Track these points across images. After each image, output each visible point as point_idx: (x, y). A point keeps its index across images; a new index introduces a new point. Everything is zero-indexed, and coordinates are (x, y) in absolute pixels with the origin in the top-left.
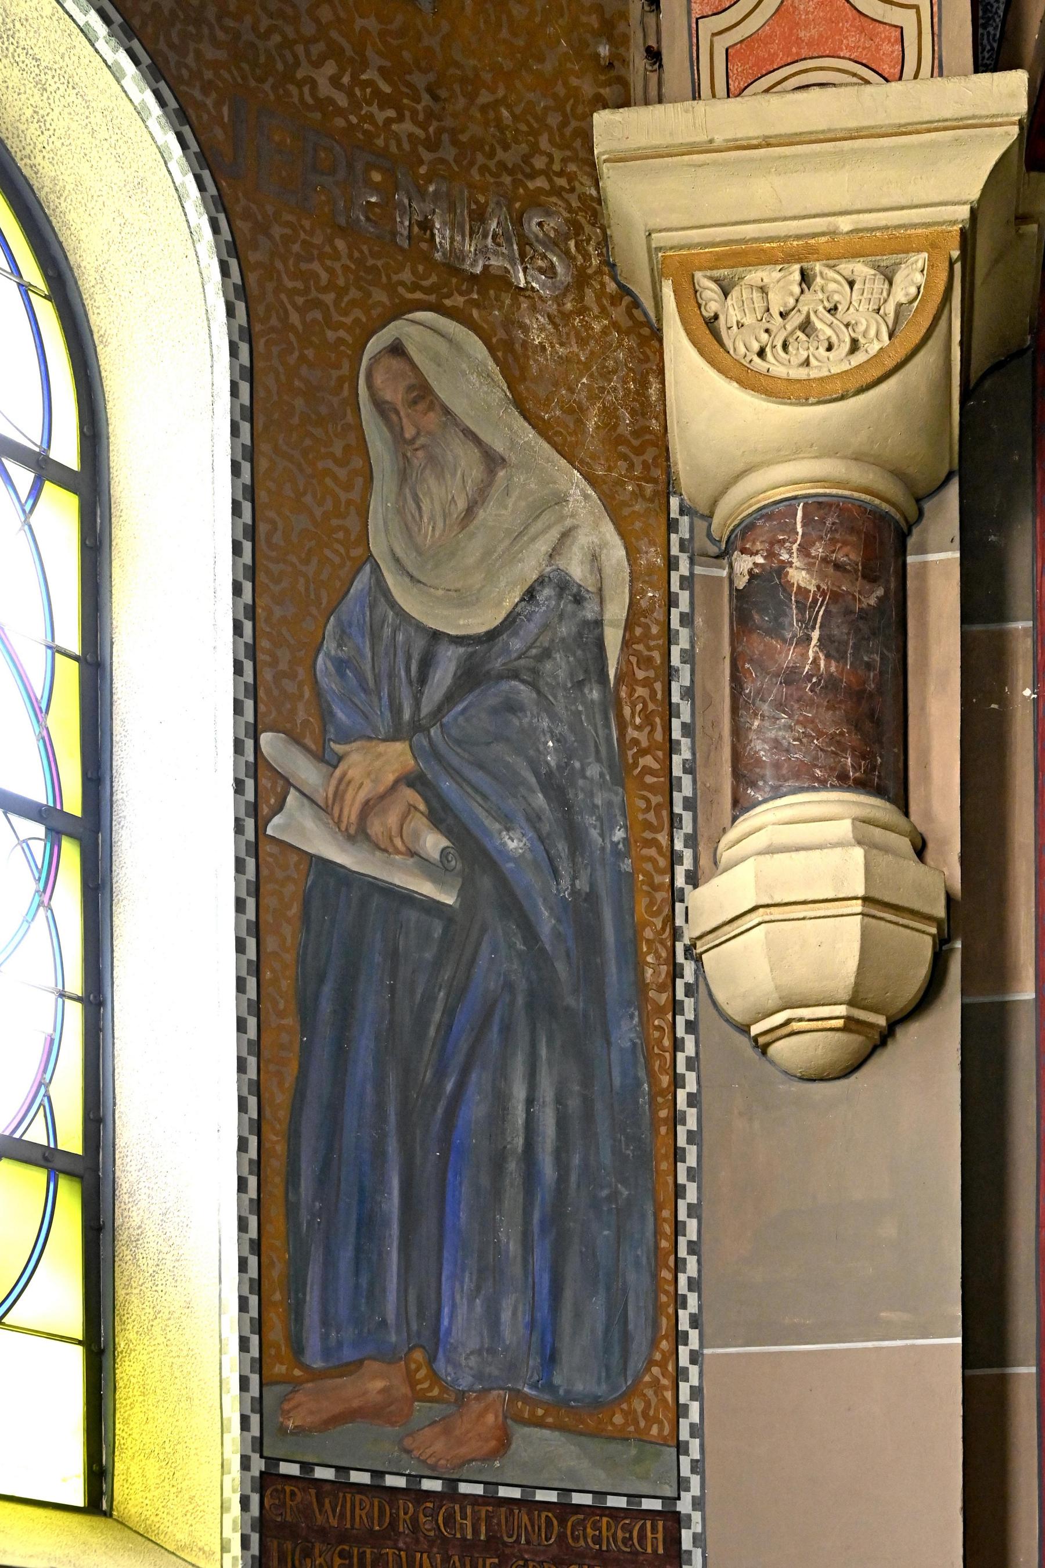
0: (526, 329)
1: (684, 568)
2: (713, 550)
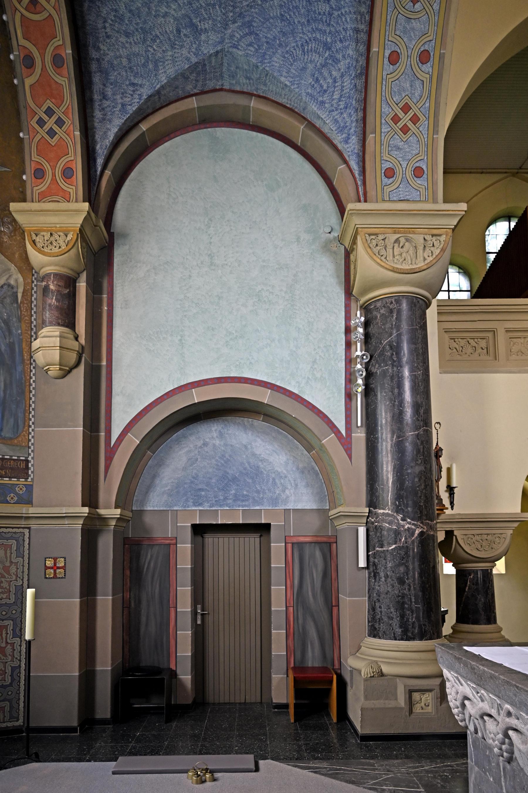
0: (3, 238)
1: (35, 283)
2: (41, 280)
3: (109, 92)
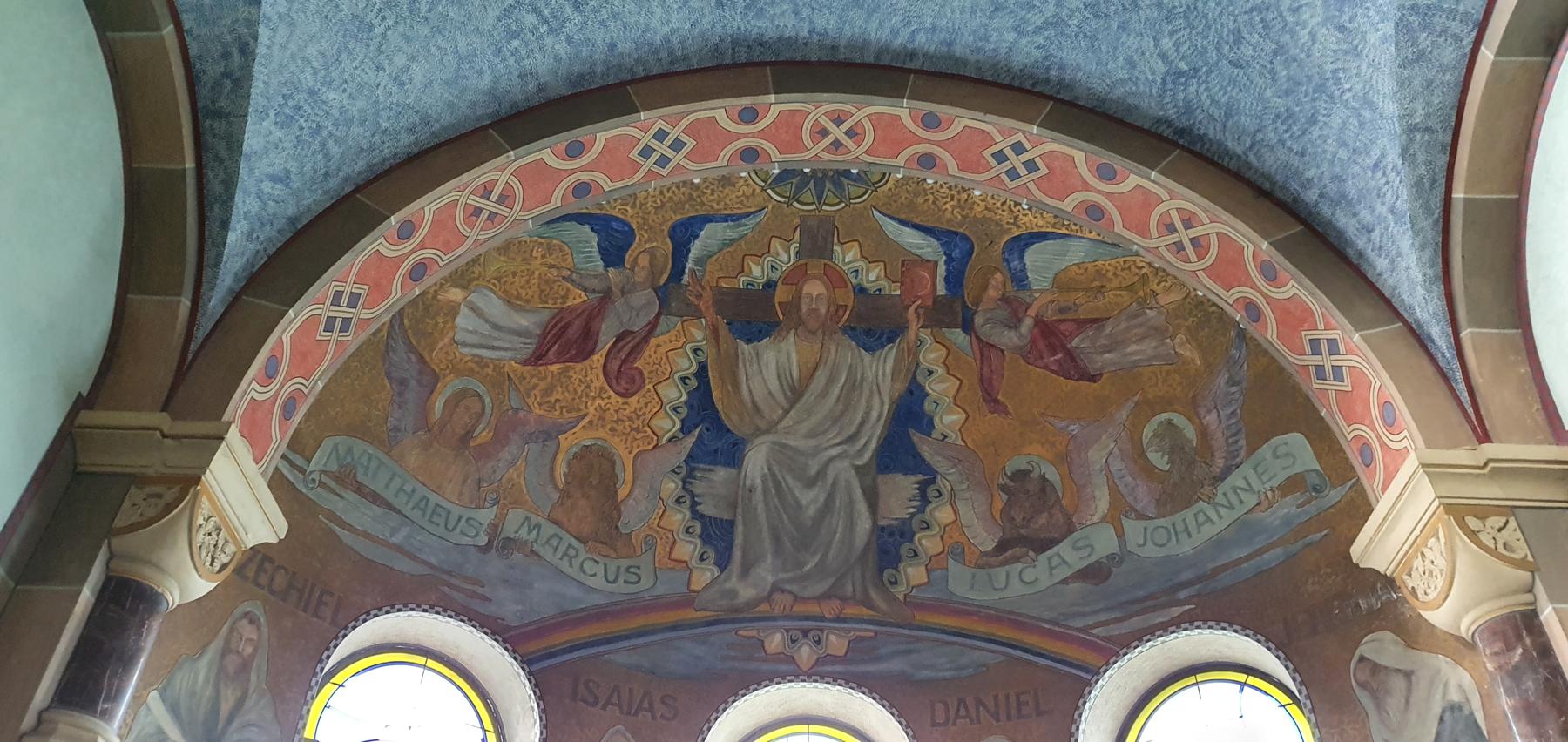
3: (1366, 216)
